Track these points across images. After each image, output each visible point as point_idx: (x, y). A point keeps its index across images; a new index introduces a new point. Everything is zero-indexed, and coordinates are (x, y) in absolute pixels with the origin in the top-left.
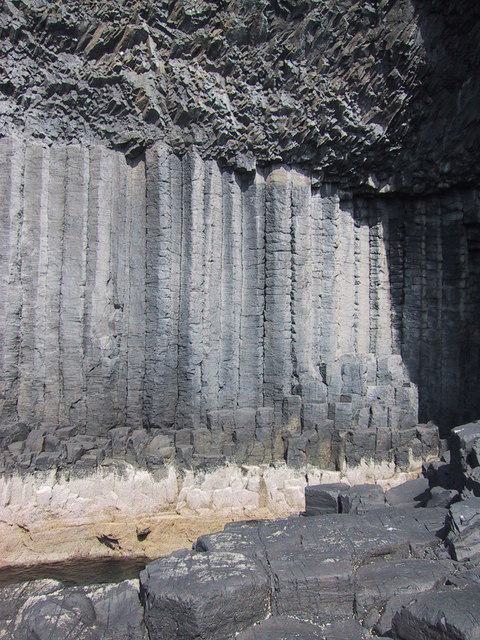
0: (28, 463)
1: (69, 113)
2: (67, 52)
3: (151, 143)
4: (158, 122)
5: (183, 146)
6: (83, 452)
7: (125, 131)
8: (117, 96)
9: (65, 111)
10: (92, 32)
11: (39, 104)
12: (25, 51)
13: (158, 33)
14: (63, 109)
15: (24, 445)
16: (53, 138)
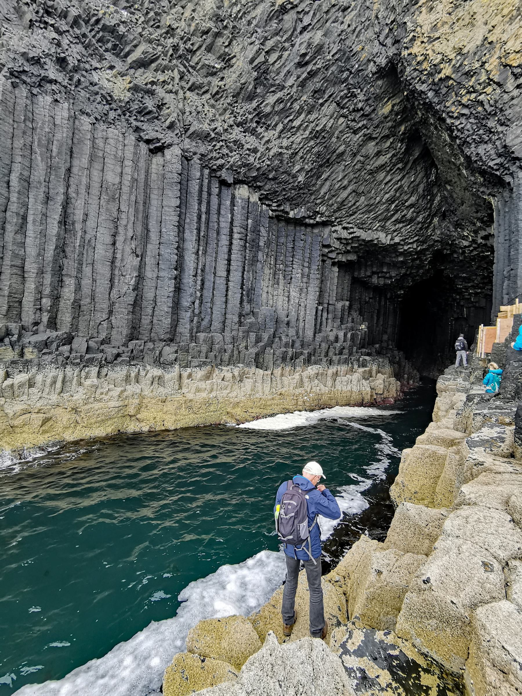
0: (78, 361)
1: (110, 104)
2: (113, 54)
3: (170, 145)
4: (176, 132)
5: (191, 154)
6: (118, 355)
7: (151, 131)
8: (150, 104)
9: (107, 101)
10: (135, 46)
11: (86, 87)
12: (77, 38)
13: (182, 69)
14: (106, 99)
15: (71, 349)
16: (96, 119)
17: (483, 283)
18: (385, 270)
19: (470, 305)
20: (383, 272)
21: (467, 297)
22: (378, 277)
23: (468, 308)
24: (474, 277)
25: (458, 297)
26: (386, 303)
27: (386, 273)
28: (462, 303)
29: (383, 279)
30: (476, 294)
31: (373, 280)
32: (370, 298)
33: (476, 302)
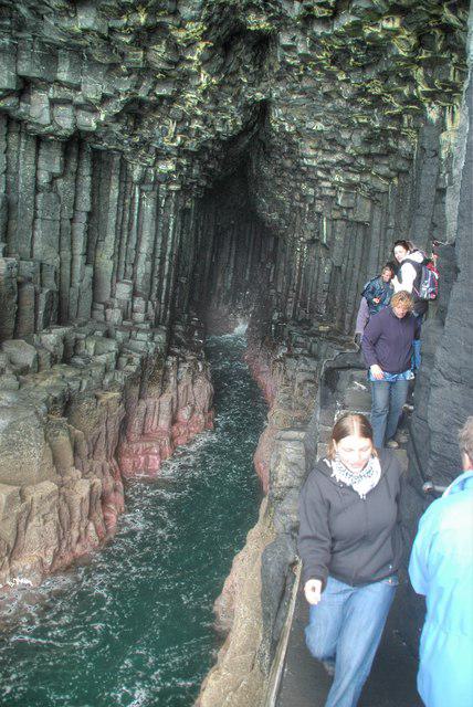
17: (367, 156)
18: (63, 76)
19: (336, 215)
20: (60, 84)
21: (328, 192)
22: (53, 103)
23: (332, 220)
24: (345, 135)
25: (311, 192)
26: (123, 195)
27: (70, 86)
28: (318, 208)
29: (68, 110)
30: (351, 186)
31: (35, 112)
32: (53, 178)
33: (348, 209)
